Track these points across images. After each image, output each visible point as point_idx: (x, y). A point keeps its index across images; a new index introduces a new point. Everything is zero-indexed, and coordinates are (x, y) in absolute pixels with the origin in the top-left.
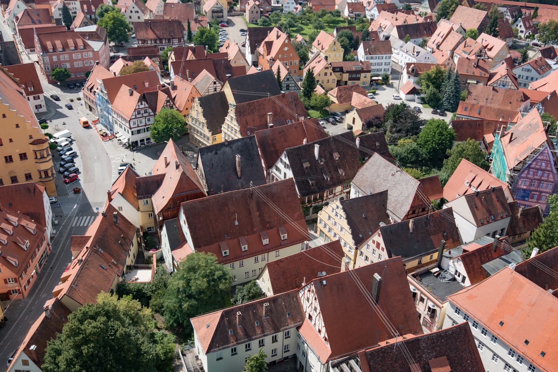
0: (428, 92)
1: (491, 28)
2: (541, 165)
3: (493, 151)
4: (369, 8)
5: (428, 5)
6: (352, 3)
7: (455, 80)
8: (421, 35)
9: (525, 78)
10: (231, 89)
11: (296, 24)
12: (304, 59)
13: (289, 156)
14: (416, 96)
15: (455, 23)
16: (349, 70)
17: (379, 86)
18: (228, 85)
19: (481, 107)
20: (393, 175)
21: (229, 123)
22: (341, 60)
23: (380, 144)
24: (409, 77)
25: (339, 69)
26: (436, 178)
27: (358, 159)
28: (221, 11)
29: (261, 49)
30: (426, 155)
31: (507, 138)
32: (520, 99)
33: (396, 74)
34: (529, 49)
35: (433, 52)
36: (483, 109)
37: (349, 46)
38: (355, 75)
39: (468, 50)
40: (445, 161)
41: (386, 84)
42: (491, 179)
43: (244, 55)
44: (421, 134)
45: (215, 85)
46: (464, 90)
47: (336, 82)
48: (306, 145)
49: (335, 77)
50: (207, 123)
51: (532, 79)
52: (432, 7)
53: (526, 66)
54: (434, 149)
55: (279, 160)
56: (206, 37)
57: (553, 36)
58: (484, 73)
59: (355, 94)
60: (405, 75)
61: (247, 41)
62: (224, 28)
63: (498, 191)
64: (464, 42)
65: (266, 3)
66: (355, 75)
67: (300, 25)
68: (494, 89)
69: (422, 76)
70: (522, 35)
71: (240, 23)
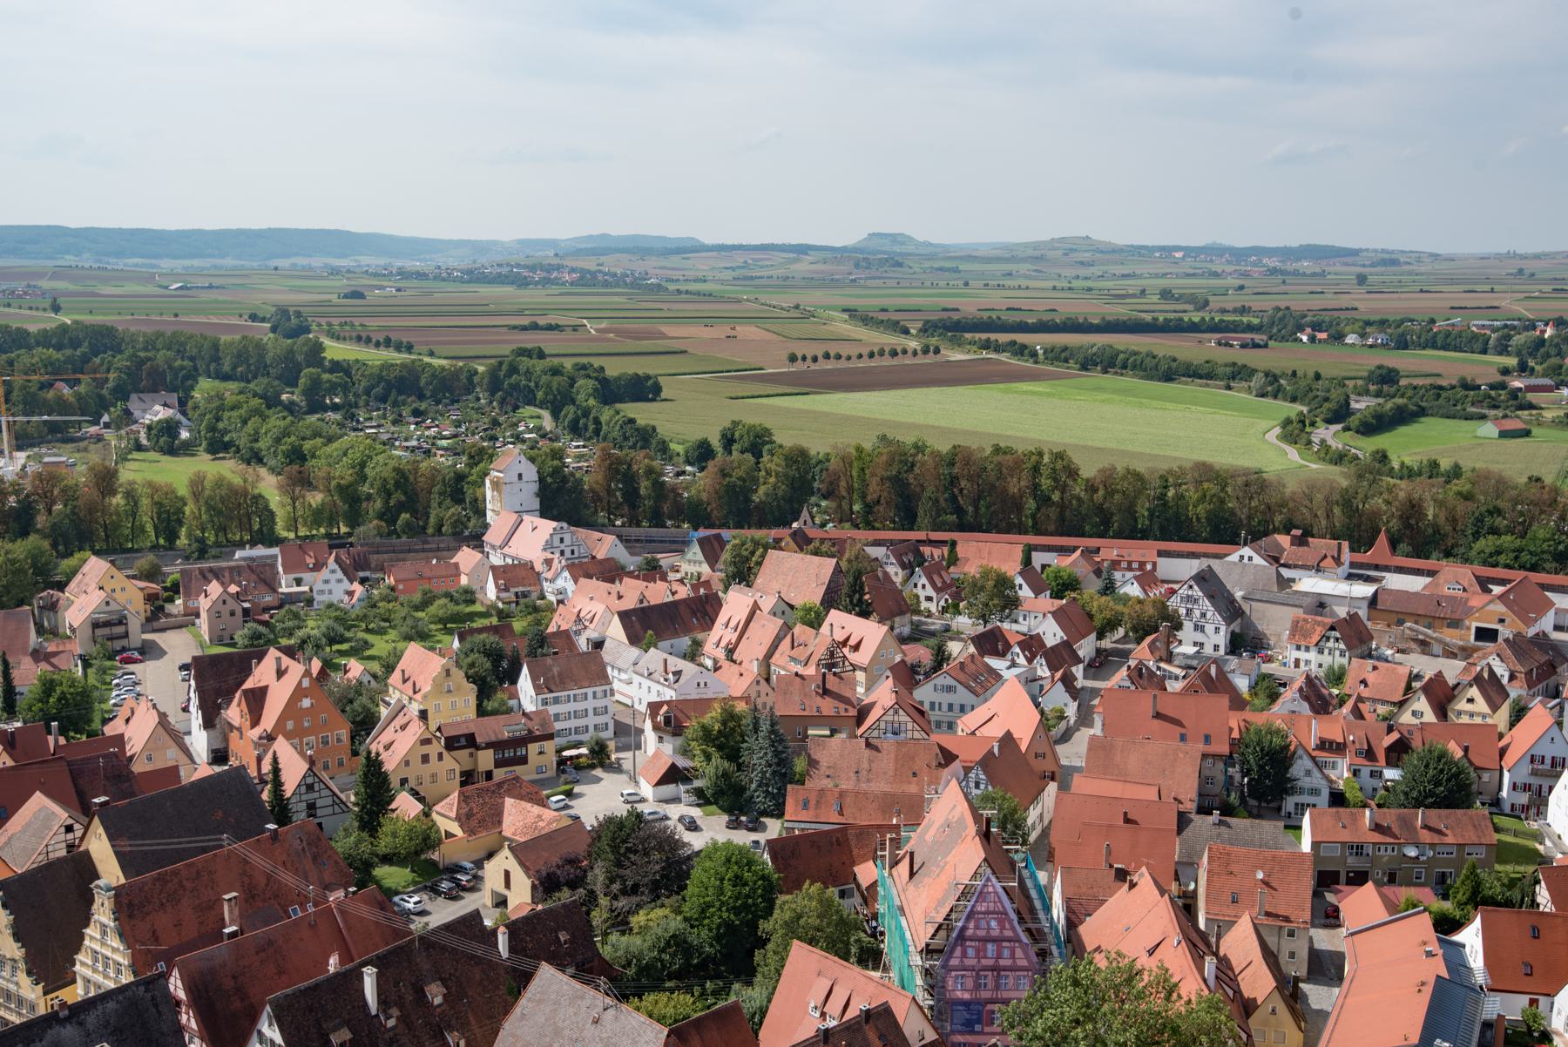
0: (710, 770)
1: (851, 597)
2: (989, 928)
3: (881, 908)
4: (549, 575)
5: (700, 556)
6: (507, 566)
7: (773, 732)
8: (687, 630)
9: (945, 707)
10: (111, 838)
11: (348, 635)
12: (364, 724)
13: (280, 1019)
14: (682, 788)
15: (767, 593)
16: (493, 739)
17: (582, 774)
18: (101, 830)
19: (842, 794)
20: (596, 1022)
21: (97, 947)
22: (472, 714)
23: (573, 935)
24: (661, 739)
25: (463, 742)
26: (736, 1008)
27: (503, 990)
28: (122, 621)
29: (234, 713)
30: (711, 945)
31: (904, 867)
32: (934, 764)
33: (627, 735)
34: (951, 639)
35: (716, 670)
36: (848, 801)
37: (491, 676)
38: (511, 751)
39: (801, 653)
40: (758, 956)
41: (602, 765)
42: (871, 987)
43: (178, 738)
44: (692, 889)
45: (70, 836)
46: (799, 755)
47: (458, 779)
48: (336, 975)
49: (452, 764)
50: (28, 958)
51: (962, 709)
52: (712, 559)
53: (942, 680)
54: (728, 924)
55: (255, 1037)
56: (59, 700)
57: (996, 601)
58: (842, 706)
59: (509, 802)
60: (650, 736)
61: (192, 694)
62: (131, 667)
63: (880, 1017)
64: (789, 637)
65: (262, 586)
66: (511, 751)
67: (361, 635)
68: (868, 745)
69: (689, 733)
70: (933, 609)
71: (180, 646)
